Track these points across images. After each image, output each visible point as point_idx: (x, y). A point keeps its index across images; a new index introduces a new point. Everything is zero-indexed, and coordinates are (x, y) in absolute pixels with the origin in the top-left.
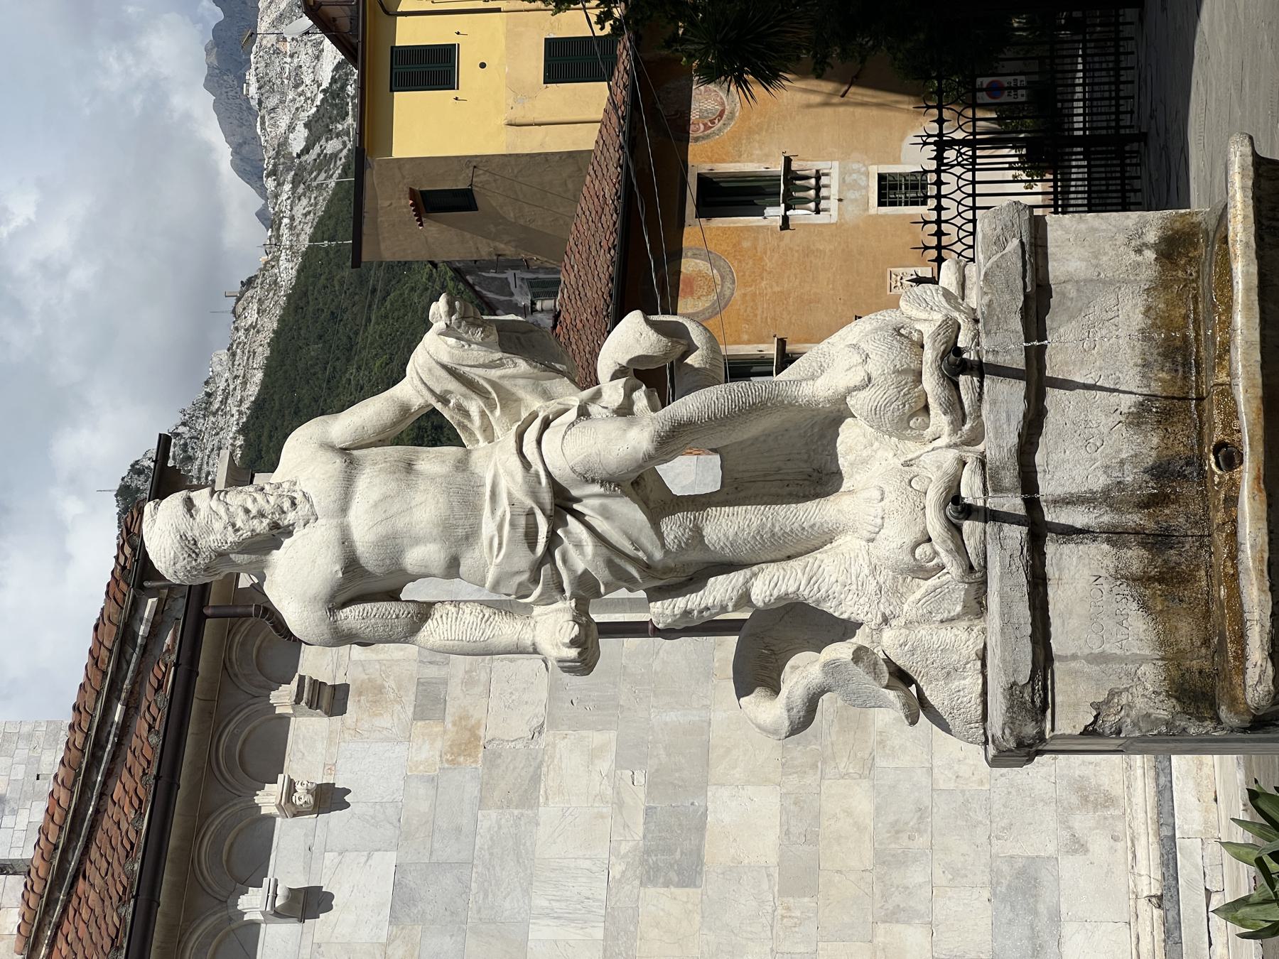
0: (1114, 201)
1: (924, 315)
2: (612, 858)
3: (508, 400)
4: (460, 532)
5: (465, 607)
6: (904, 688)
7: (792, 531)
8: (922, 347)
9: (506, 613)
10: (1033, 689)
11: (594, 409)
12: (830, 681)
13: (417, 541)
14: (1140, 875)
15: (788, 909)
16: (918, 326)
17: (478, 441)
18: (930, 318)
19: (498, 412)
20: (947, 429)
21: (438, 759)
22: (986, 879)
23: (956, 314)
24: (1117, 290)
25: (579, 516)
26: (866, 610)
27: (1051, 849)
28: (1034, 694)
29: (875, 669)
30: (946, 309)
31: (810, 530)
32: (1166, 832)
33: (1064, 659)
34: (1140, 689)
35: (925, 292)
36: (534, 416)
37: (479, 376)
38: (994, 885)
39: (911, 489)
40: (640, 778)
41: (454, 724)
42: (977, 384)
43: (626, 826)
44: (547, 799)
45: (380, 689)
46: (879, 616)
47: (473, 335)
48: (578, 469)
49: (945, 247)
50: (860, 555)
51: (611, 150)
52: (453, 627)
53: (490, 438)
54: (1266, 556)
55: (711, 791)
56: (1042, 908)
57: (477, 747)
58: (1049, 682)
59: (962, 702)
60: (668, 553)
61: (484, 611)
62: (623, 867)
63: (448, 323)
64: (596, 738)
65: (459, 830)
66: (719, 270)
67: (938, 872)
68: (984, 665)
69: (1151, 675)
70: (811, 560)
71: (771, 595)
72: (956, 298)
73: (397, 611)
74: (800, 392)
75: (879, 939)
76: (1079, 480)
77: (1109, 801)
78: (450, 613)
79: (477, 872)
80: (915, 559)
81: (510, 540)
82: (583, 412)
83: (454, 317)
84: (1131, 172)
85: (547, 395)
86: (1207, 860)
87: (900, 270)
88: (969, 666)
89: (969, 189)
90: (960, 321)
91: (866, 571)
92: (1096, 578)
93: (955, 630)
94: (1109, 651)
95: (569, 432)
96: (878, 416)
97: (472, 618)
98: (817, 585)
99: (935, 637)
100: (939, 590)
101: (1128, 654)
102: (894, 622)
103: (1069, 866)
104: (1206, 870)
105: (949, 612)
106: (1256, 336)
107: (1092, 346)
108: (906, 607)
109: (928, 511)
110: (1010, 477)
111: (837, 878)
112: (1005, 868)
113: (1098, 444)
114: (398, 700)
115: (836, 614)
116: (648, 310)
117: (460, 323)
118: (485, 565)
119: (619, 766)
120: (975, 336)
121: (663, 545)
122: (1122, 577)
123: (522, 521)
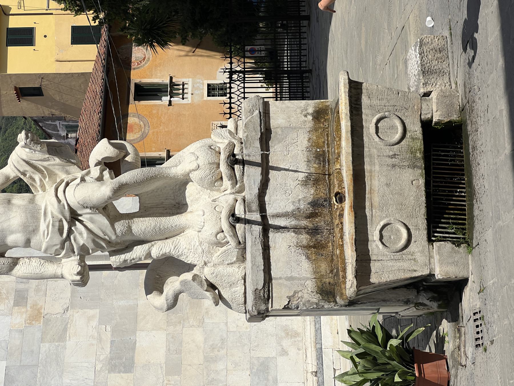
0: (300, 96)
1: (221, 141)
2: (97, 362)
3: (51, 174)
4: (31, 228)
5: (33, 259)
6: (213, 291)
7: (167, 228)
8: (220, 153)
9: (50, 262)
10: (264, 291)
11: (87, 178)
12: (183, 288)
13: (12, 232)
14: (309, 364)
15: (169, 381)
16: (218, 145)
17: (39, 191)
18: (223, 142)
19: (47, 179)
20: (230, 187)
21: (24, 322)
22: (248, 366)
23: (233, 140)
24: (297, 131)
25: (81, 222)
26: (197, 259)
27: (274, 354)
28: (264, 293)
29: (201, 283)
30: (230, 138)
31: (175, 227)
32: (318, 346)
33: (276, 279)
34: (306, 290)
35: (222, 131)
36: (62, 181)
37: (39, 165)
38: (251, 369)
39: (215, 211)
40: (109, 328)
41: (31, 308)
42: (242, 168)
43: (102, 348)
44: (70, 338)
46: (203, 262)
47: (36, 147)
48: (81, 203)
49: (233, 113)
50: (195, 237)
51: (99, 72)
52: (28, 268)
53: (44, 190)
54: (354, 237)
56: (270, 378)
57: (40, 317)
58: (270, 288)
59: (236, 297)
60: (117, 236)
61: (41, 261)
62: (101, 365)
63: (26, 142)
64: (91, 312)
65: (32, 352)
66: (143, 122)
67: (229, 364)
68: (245, 282)
69: (310, 285)
70: (175, 239)
71: (159, 254)
72: (234, 134)
73: (4, 261)
74: (171, 172)
76: (282, 207)
77: (296, 334)
78: (26, 262)
79: (40, 369)
80: (217, 239)
81: (52, 232)
82: (83, 180)
83: (28, 140)
84: (306, 84)
85: (68, 173)
86: (334, 357)
87: (216, 123)
88: (239, 282)
89: (242, 90)
90: (235, 143)
91: (197, 244)
92: (289, 246)
93: (233, 268)
94: (294, 276)
95: (77, 188)
96: (202, 181)
97: (36, 264)
98: (178, 249)
99: (225, 271)
100: (227, 252)
101: (301, 276)
102: (209, 265)
103: (281, 361)
104: (334, 361)
105: (231, 260)
106: (350, 150)
107: (288, 153)
108: (213, 258)
109: (222, 220)
110: (255, 206)
111: (189, 368)
112: (256, 362)
113: (290, 193)
114: (7, 298)
115: (185, 261)
116: (109, 139)
117: (31, 142)
118: (41, 242)
119: (100, 323)
120: (241, 149)
121: (116, 233)
122: (299, 246)
123: (57, 224)
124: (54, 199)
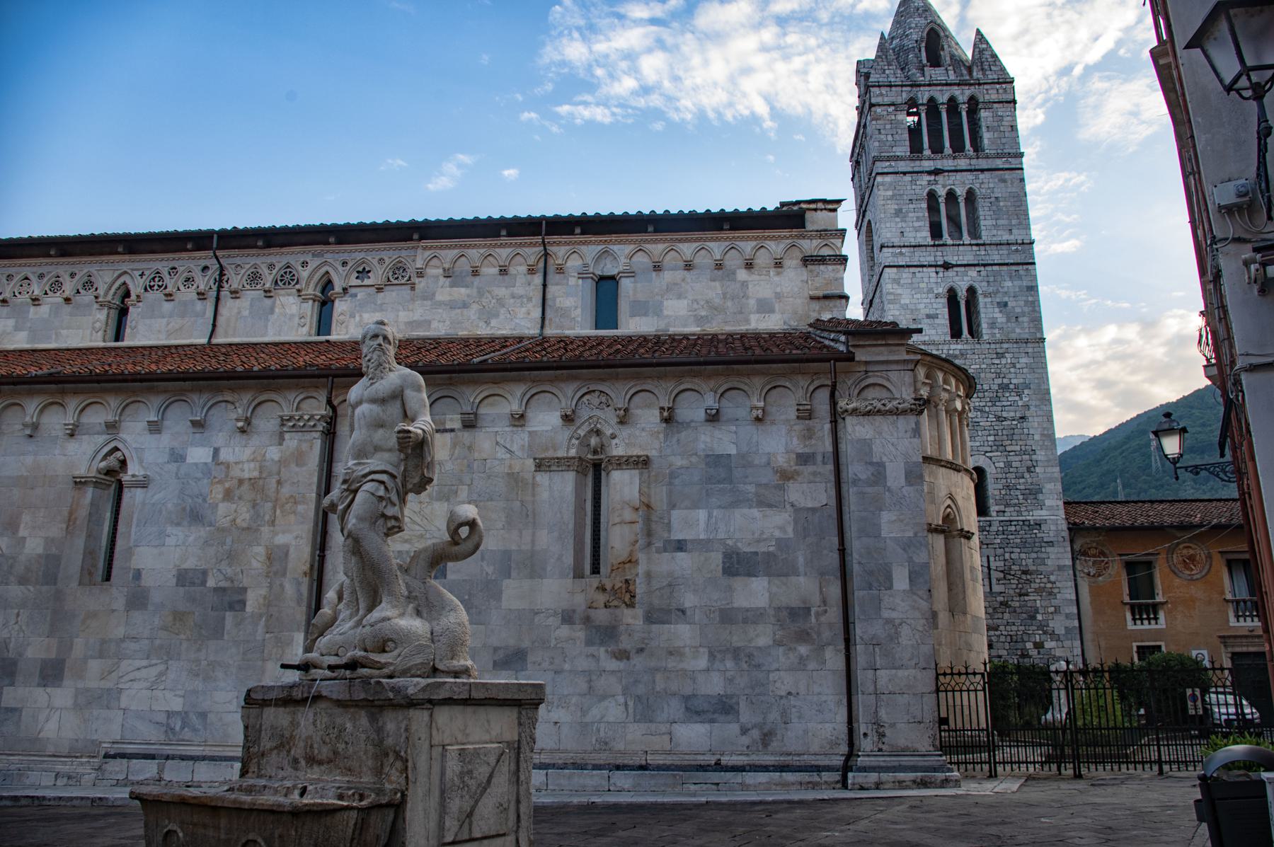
11: (384, 504)
32: (748, 768)
38: (726, 696)
40: (771, 549)
43: (749, 544)
45: (810, 438)
55: (766, 579)
56: (716, 716)
64: (790, 529)
65: (747, 477)
75: (701, 650)
77: (765, 745)
82: (381, 498)
103: (734, 728)
112: (734, 701)
114: (805, 446)
119: (777, 539)
124: (367, 470)
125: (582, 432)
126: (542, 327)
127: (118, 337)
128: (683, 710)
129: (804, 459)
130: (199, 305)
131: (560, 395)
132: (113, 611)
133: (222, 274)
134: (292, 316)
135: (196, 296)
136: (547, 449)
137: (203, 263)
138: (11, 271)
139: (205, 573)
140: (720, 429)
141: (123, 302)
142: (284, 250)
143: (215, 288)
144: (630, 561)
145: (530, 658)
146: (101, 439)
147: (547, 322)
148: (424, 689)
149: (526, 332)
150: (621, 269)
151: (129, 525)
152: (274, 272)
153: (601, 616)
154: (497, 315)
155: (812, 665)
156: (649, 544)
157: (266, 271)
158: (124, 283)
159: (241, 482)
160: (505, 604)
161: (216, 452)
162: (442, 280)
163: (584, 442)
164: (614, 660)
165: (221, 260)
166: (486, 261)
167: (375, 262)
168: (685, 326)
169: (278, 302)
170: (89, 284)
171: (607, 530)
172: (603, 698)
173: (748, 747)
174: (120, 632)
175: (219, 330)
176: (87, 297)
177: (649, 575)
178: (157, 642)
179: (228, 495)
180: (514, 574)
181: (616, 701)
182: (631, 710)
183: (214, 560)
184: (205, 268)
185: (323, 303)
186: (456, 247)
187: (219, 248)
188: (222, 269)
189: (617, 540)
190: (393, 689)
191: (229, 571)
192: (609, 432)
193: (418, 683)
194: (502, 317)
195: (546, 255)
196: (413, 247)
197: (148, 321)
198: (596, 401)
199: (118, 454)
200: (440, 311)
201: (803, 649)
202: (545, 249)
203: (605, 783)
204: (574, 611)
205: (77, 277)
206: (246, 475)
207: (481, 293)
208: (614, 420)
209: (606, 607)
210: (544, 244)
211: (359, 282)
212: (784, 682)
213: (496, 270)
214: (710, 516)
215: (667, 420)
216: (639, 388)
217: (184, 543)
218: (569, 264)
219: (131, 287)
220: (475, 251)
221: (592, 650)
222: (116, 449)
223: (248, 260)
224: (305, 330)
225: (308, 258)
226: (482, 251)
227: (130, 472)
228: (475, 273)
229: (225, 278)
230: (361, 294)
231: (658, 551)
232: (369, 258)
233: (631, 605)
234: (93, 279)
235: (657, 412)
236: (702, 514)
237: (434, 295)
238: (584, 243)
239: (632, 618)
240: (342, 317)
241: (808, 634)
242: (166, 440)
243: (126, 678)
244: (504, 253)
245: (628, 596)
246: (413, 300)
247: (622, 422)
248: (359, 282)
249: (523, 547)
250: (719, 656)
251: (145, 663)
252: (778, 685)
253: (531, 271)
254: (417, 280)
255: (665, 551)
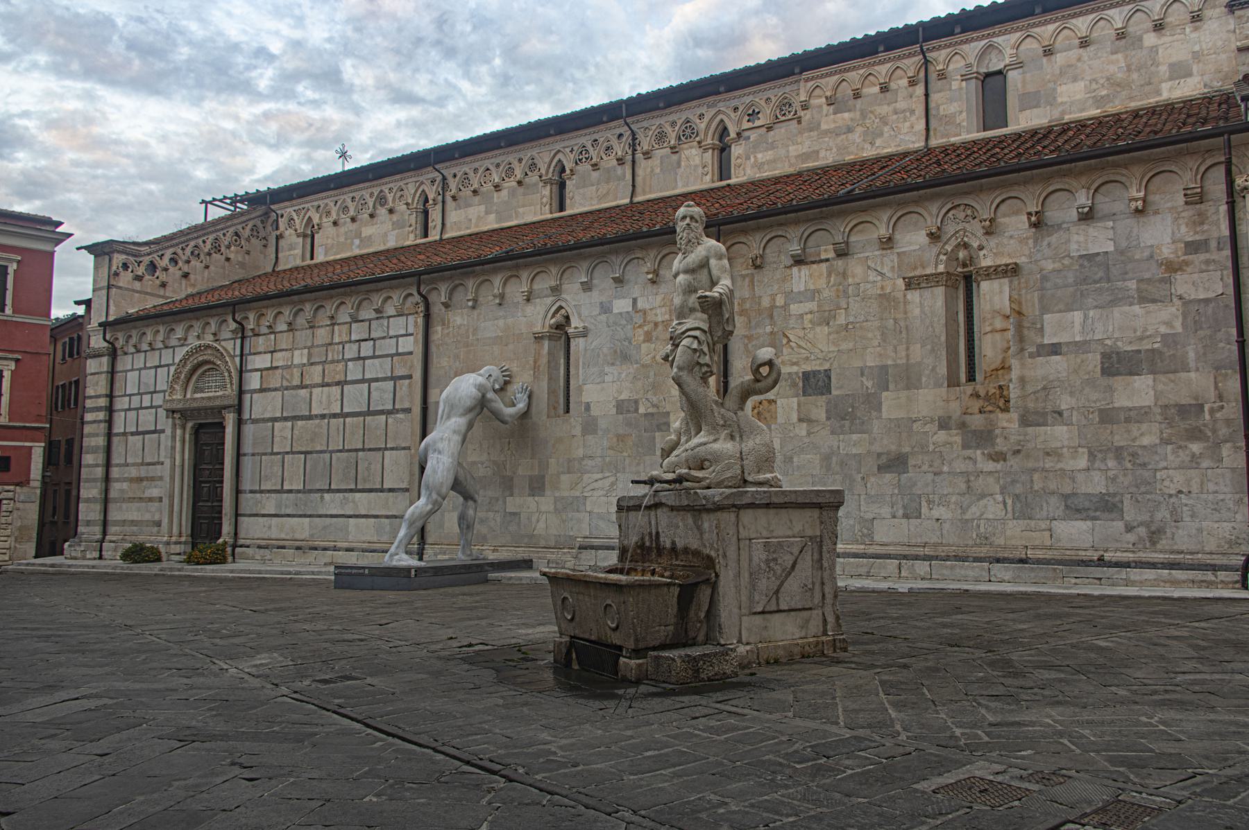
22: (1111, 491)
27: (1127, 518)
32: (1133, 565)
38: (1108, 494)
40: (1156, 346)
43: (1131, 343)
56: (1098, 513)
67: (1113, 472)
75: (1080, 450)
77: (1154, 543)
103: (1120, 525)
111: (1109, 431)
112: (1117, 499)
119: (1162, 335)
125: (949, 248)
126: (927, 139)
127: (562, 208)
128: (1063, 507)
129: (1193, 247)
130: (619, 170)
131: (925, 214)
132: (574, 436)
133: (634, 139)
134: (696, 166)
135: (615, 162)
136: (916, 268)
137: (618, 131)
138: (476, 165)
139: (636, 402)
140: (1094, 227)
141: (561, 177)
142: (683, 106)
143: (630, 152)
144: (1003, 368)
145: (911, 462)
146: (549, 300)
147: (932, 133)
148: (728, 497)
149: (911, 146)
150: (1007, 61)
151: (577, 367)
152: (677, 128)
153: (977, 421)
154: (881, 134)
155: (1205, 464)
156: (1022, 350)
157: (670, 129)
158: (560, 161)
159: (656, 324)
160: (884, 415)
161: (635, 301)
162: (825, 107)
163: (952, 257)
164: (991, 462)
165: (632, 126)
166: (867, 81)
167: (763, 103)
168: (1083, 110)
169: (683, 156)
170: (533, 166)
171: (980, 339)
172: (983, 496)
173: (1134, 544)
174: (580, 452)
175: (639, 189)
176: (533, 178)
177: (1022, 380)
178: (608, 459)
179: (648, 338)
180: (891, 386)
181: (994, 499)
182: (1009, 509)
183: (642, 392)
184: (620, 136)
185: (722, 150)
186: (835, 73)
187: (628, 116)
188: (633, 134)
189: (989, 350)
190: (705, 497)
191: (655, 400)
192: (975, 245)
193: (723, 493)
194: (886, 135)
195: (927, 62)
196: (796, 81)
197: (581, 191)
198: (962, 215)
199: (563, 311)
200: (827, 139)
201: (1195, 447)
202: (925, 57)
203: (985, 574)
204: (950, 418)
205: (524, 162)
206: (660, 319)
207: (864, 116)
208: (980, 232)
209: (980, 412)
210: (923, 52)
211: (750, 125)
212: (1173, 480)
213: (877, 89)
214: (1086, 317)
215: (1036, 225)
216: (1004, 196)
217: (618, 380)
218: (951, 67)
219: (565, 163)
220: (854, 73)
221: (969, 452)
222: (561, 308)
223: (653, 121)
224: (708, 178)
225: (703, 110)
226: (861, 72)
227: (573, 326)
228: (857, 95)
229: (637, 141)
230: (753, 136)
231: (1031, 356)
232: (757, 100)
233: (1006, 410)
234: (535, 161)
235: (1025, 218)
236: (1077, 316)
237: (819, 125)
238: (967, 42)
239: (1008, 422)
240: (739, 161)
241: (1200, 431)
242: (596, 297)
243: (588, 488)
244: (884, 69)
245: (1002, 401)
246: (801, 133)
247: (988, 233)
248: (750, 125)
249: (899, 362)
250: (1100, 456)
251: (600, 476)
252: (1166, 483)
253: (912, 83)
254: (801, 113)
255: (1039, 356)
